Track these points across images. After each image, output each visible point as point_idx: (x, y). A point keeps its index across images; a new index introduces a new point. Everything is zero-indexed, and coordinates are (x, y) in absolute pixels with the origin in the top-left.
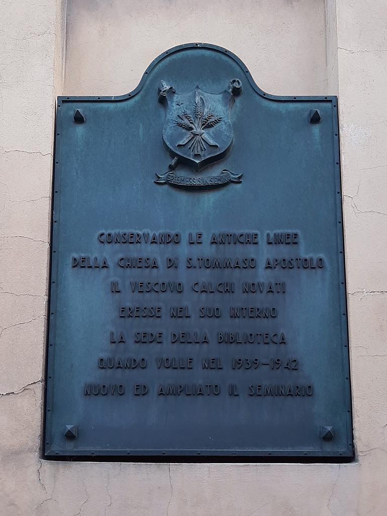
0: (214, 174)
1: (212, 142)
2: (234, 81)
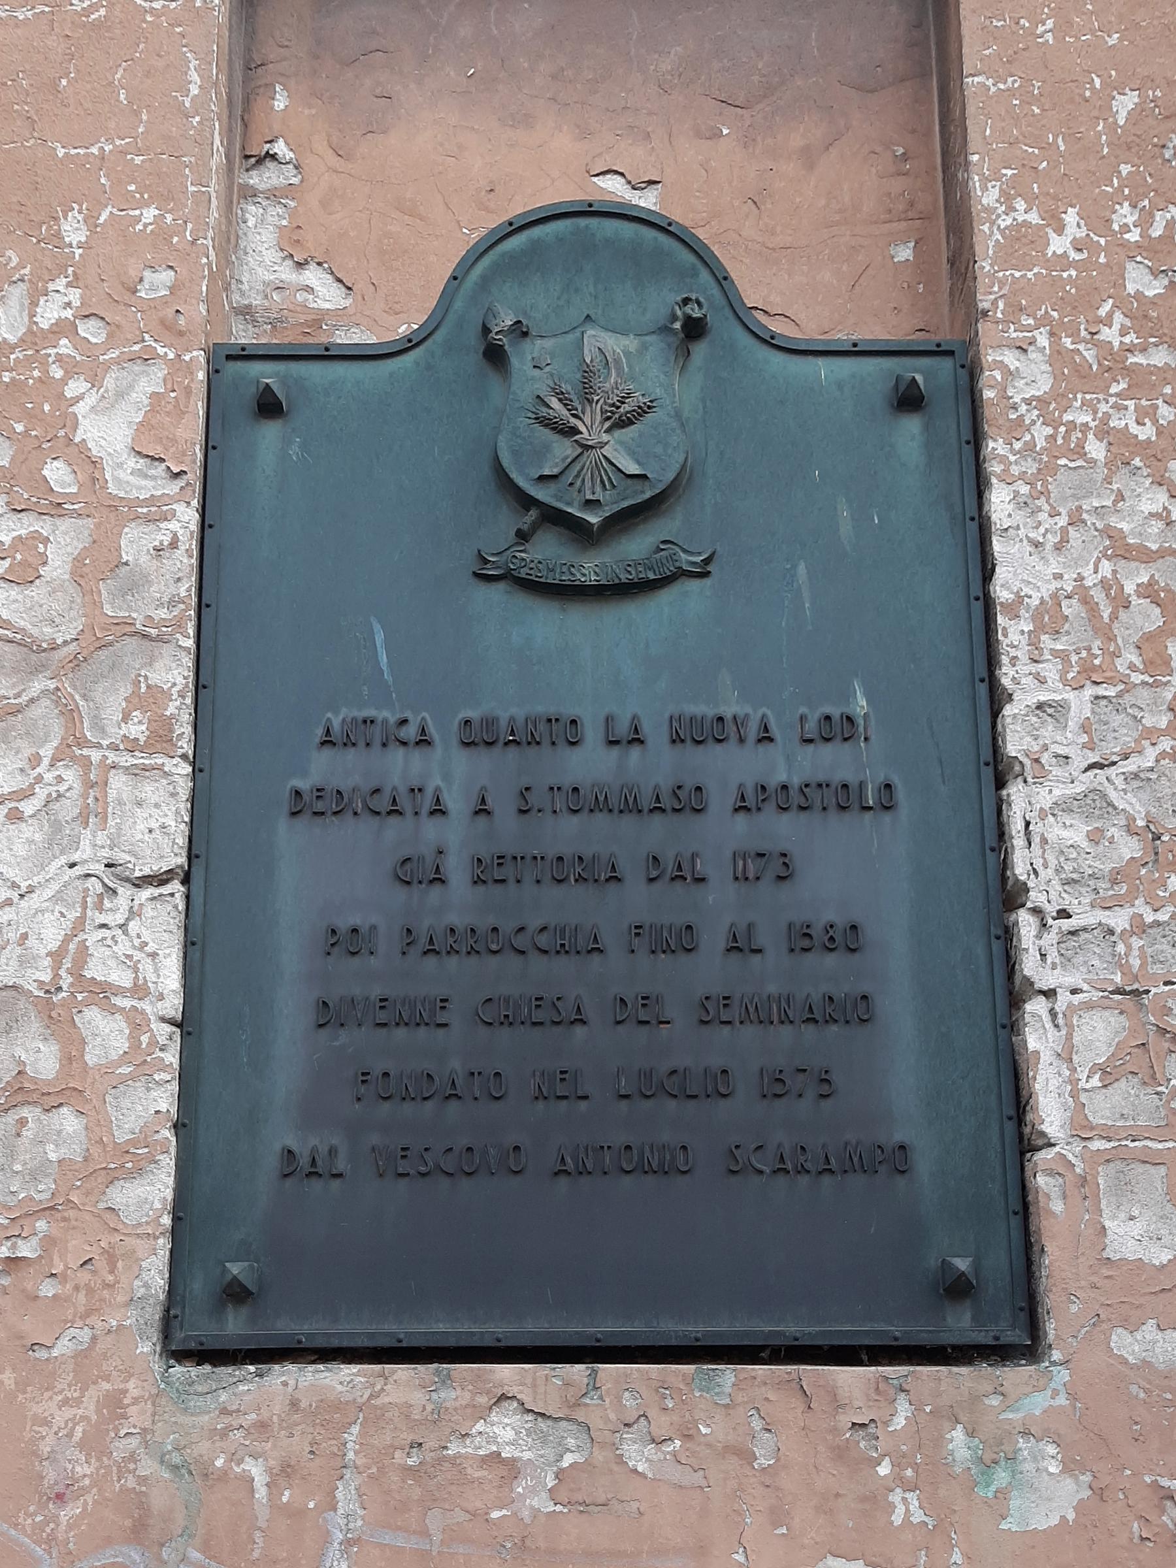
0: (635, 548)
1: (633, 469)
2: (686, 301)
